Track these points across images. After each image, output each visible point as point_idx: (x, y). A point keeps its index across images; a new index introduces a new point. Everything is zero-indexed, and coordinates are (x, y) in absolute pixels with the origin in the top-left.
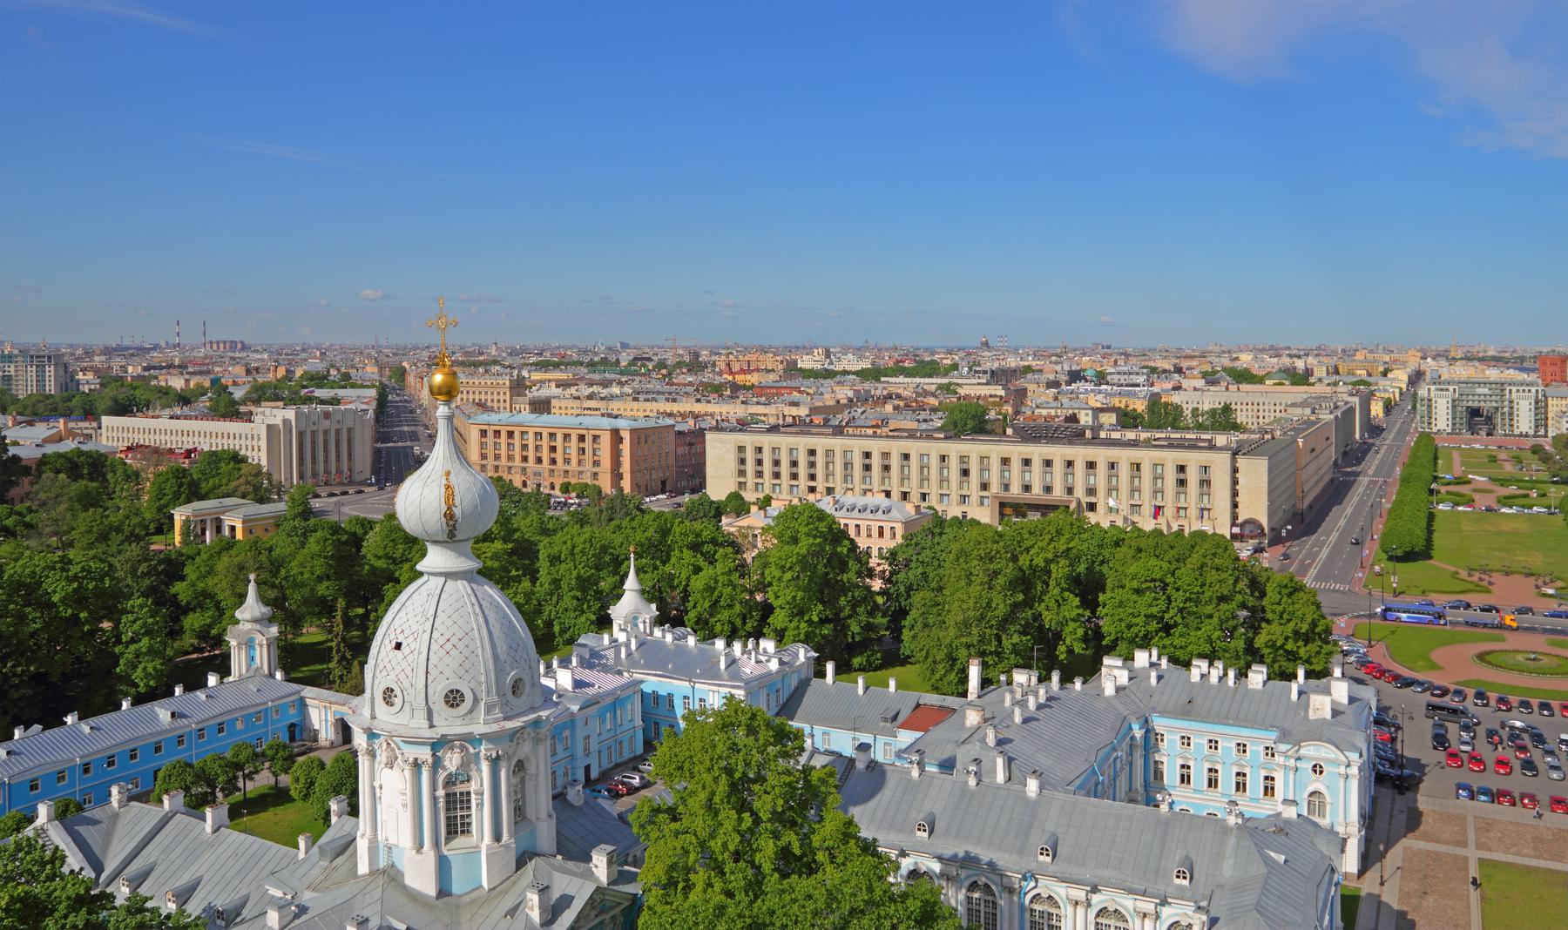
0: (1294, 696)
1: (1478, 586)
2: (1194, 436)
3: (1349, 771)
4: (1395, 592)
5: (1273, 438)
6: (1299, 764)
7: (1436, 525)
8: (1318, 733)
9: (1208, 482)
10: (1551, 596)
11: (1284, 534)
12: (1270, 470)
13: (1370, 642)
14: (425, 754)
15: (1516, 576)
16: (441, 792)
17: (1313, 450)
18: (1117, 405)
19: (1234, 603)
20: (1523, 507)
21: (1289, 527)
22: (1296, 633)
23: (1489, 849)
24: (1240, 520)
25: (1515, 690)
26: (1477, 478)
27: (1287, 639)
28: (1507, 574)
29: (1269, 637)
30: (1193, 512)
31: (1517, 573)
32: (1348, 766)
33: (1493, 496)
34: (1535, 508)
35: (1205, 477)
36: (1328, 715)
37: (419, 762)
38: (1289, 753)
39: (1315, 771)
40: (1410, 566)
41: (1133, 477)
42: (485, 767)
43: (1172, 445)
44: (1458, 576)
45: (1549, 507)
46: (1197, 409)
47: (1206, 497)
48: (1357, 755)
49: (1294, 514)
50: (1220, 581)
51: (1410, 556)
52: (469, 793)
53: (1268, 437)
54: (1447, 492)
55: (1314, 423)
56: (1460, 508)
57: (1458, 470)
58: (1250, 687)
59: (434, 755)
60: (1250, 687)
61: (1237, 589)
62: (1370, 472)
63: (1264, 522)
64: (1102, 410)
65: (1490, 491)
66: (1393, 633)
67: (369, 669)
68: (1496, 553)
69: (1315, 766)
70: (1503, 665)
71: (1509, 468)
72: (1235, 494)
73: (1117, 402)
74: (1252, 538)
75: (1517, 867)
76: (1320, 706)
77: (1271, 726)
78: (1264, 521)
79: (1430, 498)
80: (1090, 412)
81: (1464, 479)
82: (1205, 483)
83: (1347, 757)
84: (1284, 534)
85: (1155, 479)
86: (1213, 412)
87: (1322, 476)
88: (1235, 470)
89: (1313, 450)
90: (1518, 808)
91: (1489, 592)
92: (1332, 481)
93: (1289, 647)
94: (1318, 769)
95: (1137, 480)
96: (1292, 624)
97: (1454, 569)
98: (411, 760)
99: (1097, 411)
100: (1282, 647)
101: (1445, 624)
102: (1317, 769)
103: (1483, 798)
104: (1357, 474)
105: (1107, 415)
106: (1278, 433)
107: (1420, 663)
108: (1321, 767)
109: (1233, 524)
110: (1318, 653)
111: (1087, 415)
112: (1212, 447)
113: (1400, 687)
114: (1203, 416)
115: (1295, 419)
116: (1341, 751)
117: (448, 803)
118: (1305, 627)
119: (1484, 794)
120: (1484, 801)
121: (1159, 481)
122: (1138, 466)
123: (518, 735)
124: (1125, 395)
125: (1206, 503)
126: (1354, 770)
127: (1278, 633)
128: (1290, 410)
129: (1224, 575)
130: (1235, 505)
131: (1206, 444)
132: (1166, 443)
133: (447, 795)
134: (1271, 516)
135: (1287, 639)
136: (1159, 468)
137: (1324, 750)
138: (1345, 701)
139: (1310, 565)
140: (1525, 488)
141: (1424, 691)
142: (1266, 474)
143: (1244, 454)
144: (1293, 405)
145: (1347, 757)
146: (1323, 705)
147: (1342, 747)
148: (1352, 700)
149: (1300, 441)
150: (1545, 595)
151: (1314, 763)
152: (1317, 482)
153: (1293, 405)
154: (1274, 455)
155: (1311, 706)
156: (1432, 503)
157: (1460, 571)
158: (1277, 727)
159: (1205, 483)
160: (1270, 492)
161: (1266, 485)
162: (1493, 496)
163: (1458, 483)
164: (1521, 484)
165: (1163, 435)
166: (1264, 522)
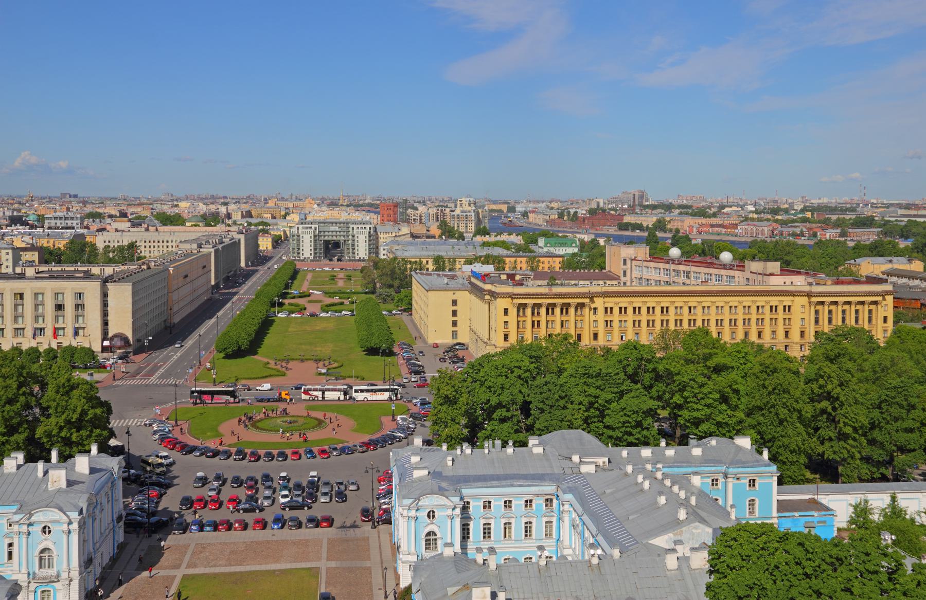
0: (40, 474)
1: (278, 371)
2: (73, 269)
3: (71, 527)
4: (215, 382)
5: (149, 268)
6: (30, 528)
7: (273, 329)
8: (53, 501)
9: (83, 306)
10: (324, 374)
11: (146, 344)
12: (134, 294)
13: (176, 422)
15: (309, 362)
17: (186, 276)
18: (46, 245)
19: (18, 405)
20: (336, 311)
21: (150, 338)
22: (68, 422)
23: (195, 566)
24: (110, 335)
25: (274, 445)
26: (315, 292)
27: (61, 428)
28: (302, 361)
29: (45, 428)
30: (70, 331)
31: (310, 359)
32: (70, 523)
33: (319, 305)
34: (343, 312)
35: (79, 302)
36: (63, 484)
38: (22, 522)
39: (45, 532)
40: (239, 360)
41: (16, 306)
43: (52, 277)
44: (269, 366)
45: (353, 311)
46: (109, 247)
47: (81, 319)
48: (77, 513)
49: (166, 328)
50: (6, 387)
51: (238, 353)
53: (145, 267)
54: (290, 304)
55: (195, 255)
56: (293, 315)
57: (304, 288)
58: (6, 471)
60: (6, 471)
61: (21, 392)
62: (242, 292)
63: (130, 335)
64: (25, 249)
65: (320, 301)
66: (201, 414)
68: (303, 346)
69: (45, 527)
70: (266, 428)
71: (341, 283)
72: (105, 314)
73: (44, 243)
74: (120, 348)
75: (215, 575)
76: (58, 477)
77: (14, 501)
78: (129, 335)
79: (272, 309)
80: (10, 251)
81: (308, 294)
82: (79, 306)
83: (68, 516)
84: (146, 344)
85: (36, 306)
86: (121, 249)
87: (198, 297)
88: (105, 295)
89: (186, 276)
90: (232, 532)
91: (284, 375)
92: (208, 300)
93: (63, 434)
94: (47, 530)
95: (20, 308)
96: (63, 417)
97: (266, 360)
99: (17, 252)
100: (58, 436)
101: (239, 402)
102: (45, 530)
103: (208, 529)
104: (235, 294)
105: (30, 253)
106: (153, 264)
107: (209, 434)
108: (49, 528)
109: (105, 338)
110: (89, 436)
111: (7, 253)
112: (88, 276)
113: (185, 454)
114: (114, 252)
115: (179, 252)
116: (65, 513)
118: (75, 417)
119: (209, 525)
120: (208, 531)
121: (40, 308)
122: (21, 296)
124: (53, 236)
125: (80, 323)
126: (75, 526)
127: (54, 424)
128: (181, 246)
129: (9, 382)
130: (105, 323)
131: (82, 275)
132: (47, 275)
134: (135, 331)
135: (61, 428)
136: (60, 296)
137: (51, 513)
138: (87, 471)
139: (161, 366)
140: (344, 298)
141: (202, 455)
142: (130, 297)
143: (115, 281)
144: (186, 242)
145: (68, 516)
146: (59, 477)
147: (65, 510)
148: (93, 471)
149: (171, 269)
150: (320, 374)
151: (43, 525)
152: (193, 301)
153: (186, 242)
154: (139, 281)
155: (50, 480)
156: (275, 312)
157: (270, 362)
158: (18, 501)
159: (79, 306)
160: (134, 312)
161: (130, 306)
162: (319, 305)
163: (300, 297)
164: (342, 295)
165: (46, 269)
166: (130, 335)
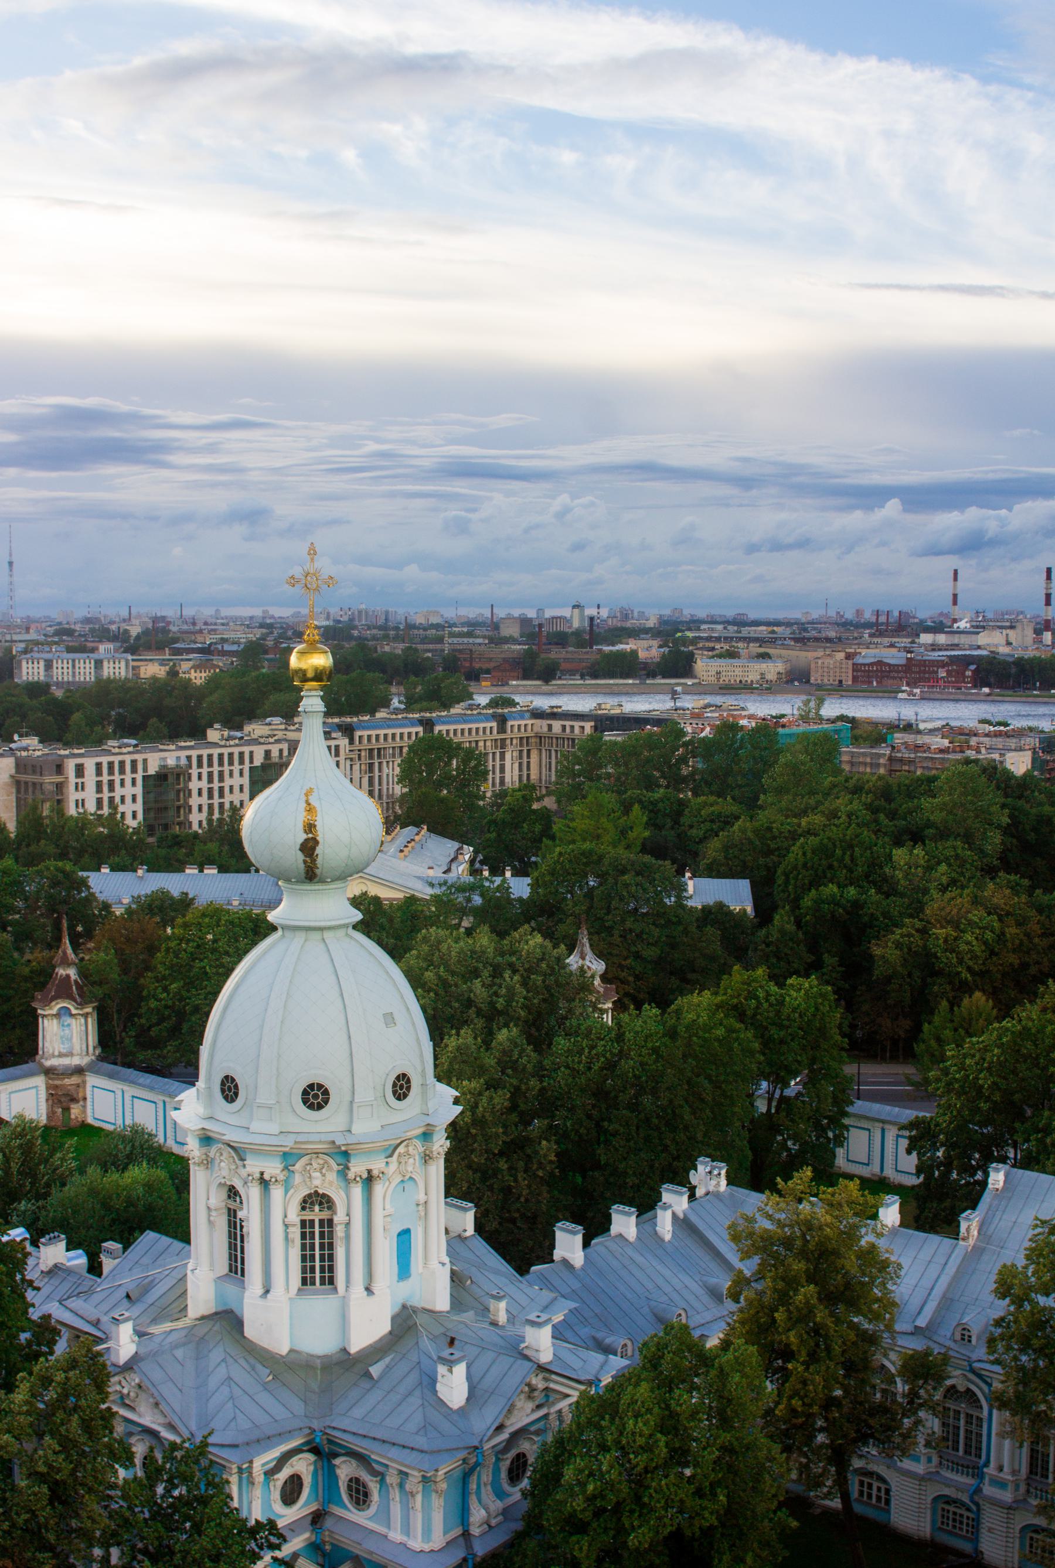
14: (273, 1168)
16: (294, 1216)
37: (266, 1177)
42: (357, 1191)
52: (330, 1222)
59: (286, 1168)
67: (204, 1050)
98: (258, 1175)
117: (303, 1236)
123: (401, 1149)
133: (303, 1223)
